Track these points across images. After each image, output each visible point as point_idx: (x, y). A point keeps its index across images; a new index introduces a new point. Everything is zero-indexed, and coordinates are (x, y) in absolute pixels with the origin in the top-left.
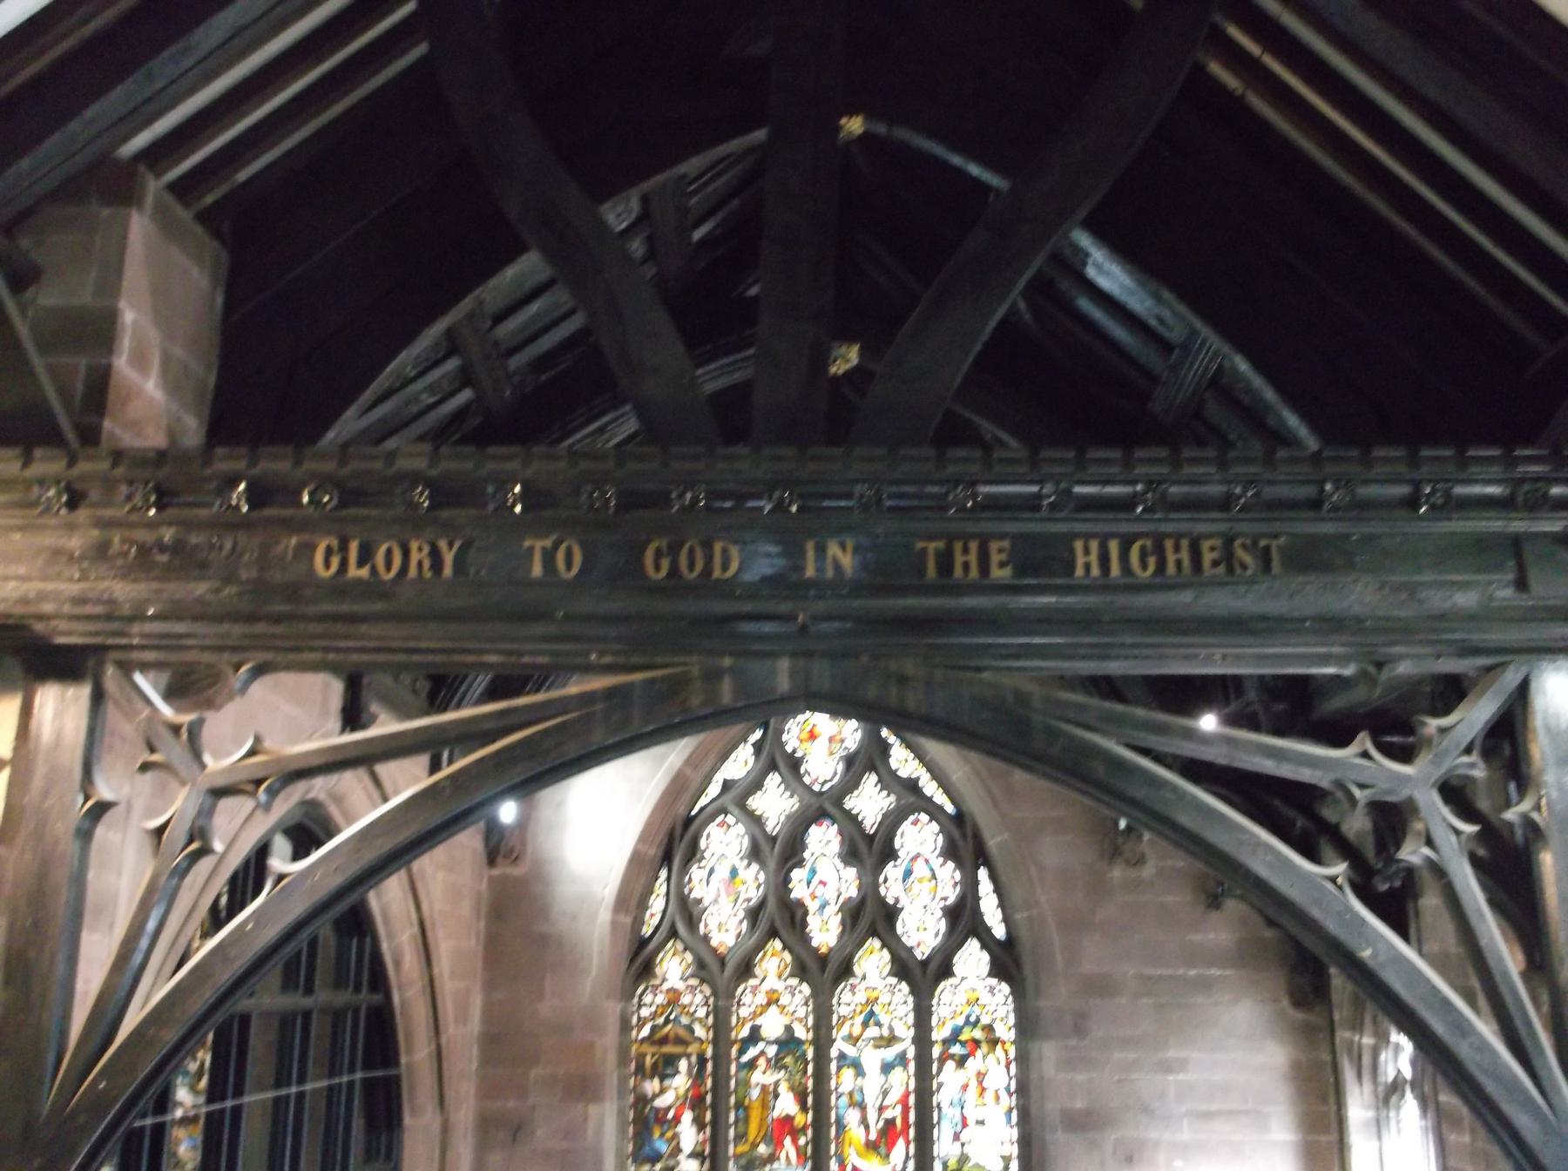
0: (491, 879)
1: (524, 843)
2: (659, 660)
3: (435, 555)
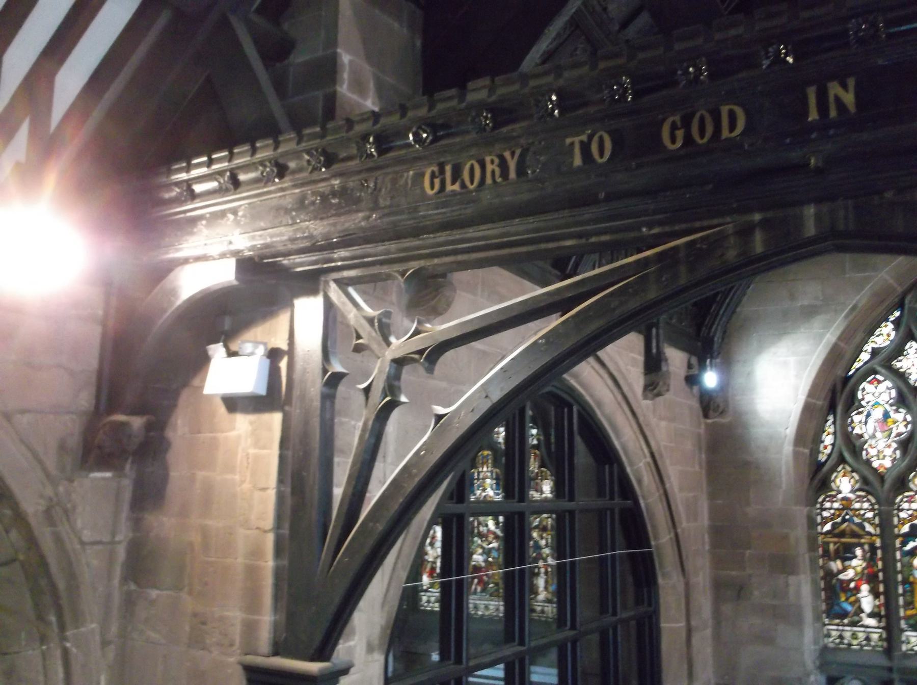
0: (707, 425)
1: (726, 402)
2: (698, 224)
3: (503, 165)
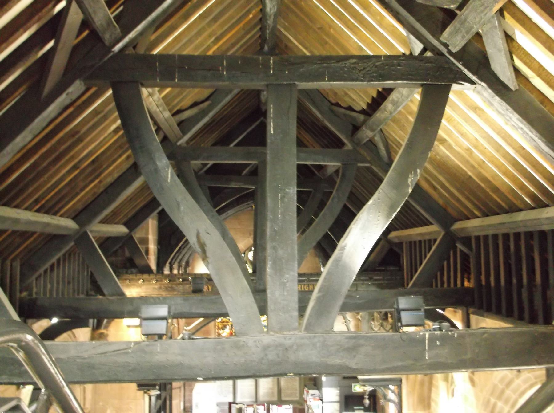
3: (208, 288)
